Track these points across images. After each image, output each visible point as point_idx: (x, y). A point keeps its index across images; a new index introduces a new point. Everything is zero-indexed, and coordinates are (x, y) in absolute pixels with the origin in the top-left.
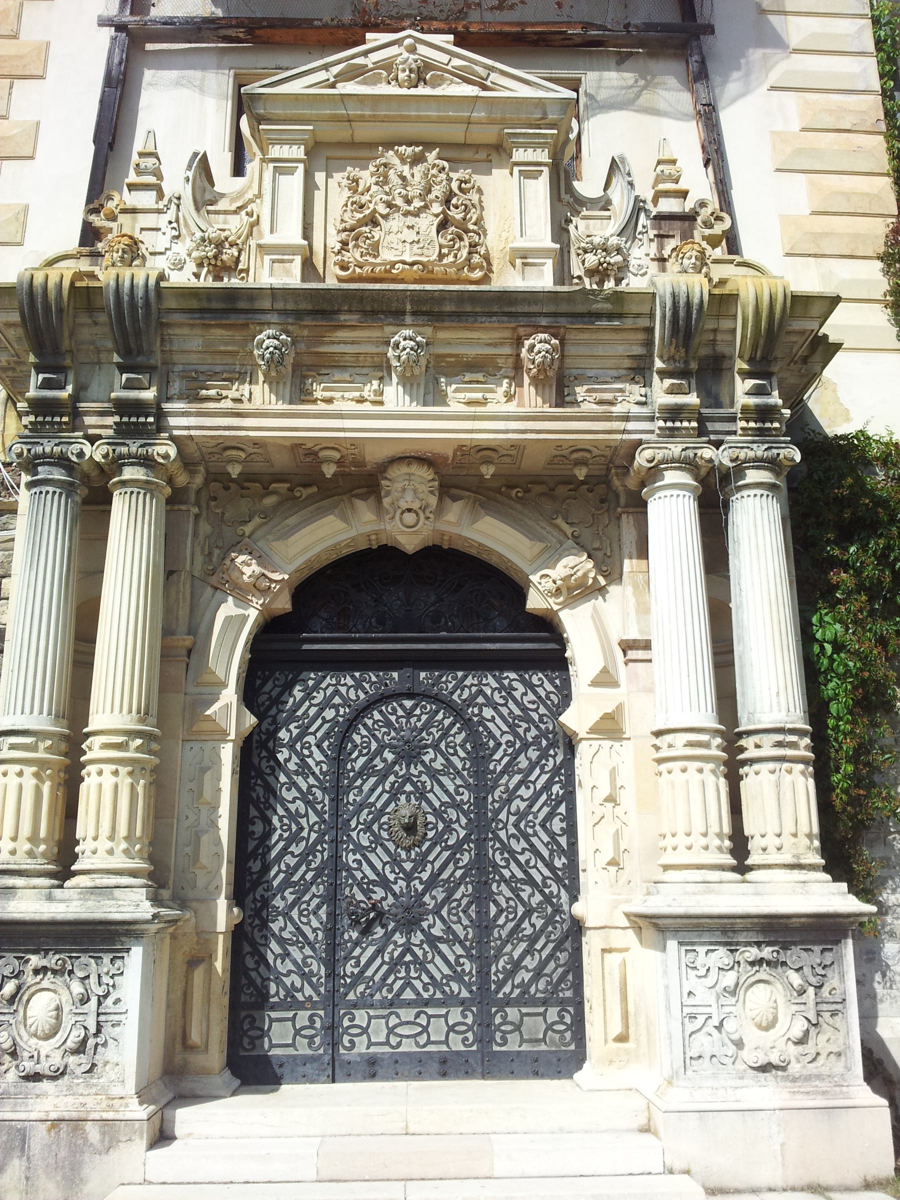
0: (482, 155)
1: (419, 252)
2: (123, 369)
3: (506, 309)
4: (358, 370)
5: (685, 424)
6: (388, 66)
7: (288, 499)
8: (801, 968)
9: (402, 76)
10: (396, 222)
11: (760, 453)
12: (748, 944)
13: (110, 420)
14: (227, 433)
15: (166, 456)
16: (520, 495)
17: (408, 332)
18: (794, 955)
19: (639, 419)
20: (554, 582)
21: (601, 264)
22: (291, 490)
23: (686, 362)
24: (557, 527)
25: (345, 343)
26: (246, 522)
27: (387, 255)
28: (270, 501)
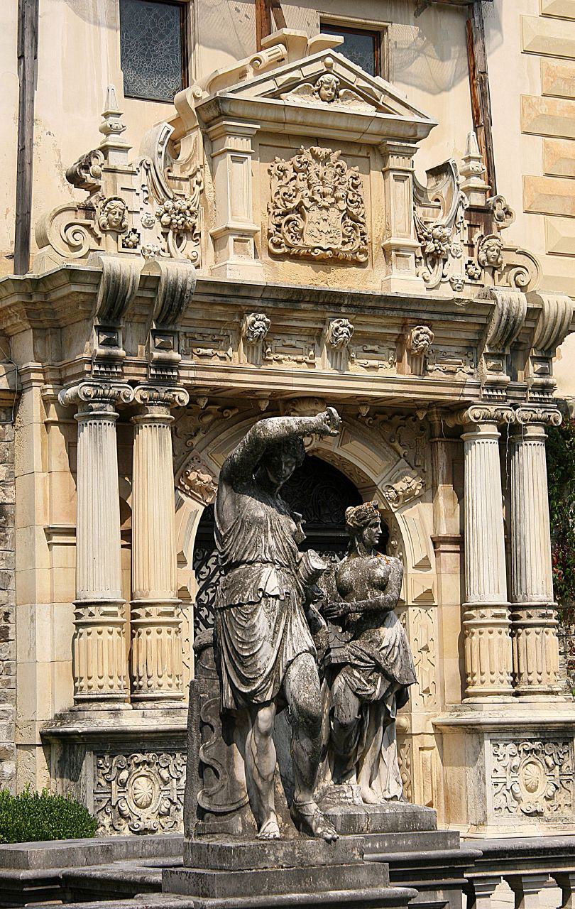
0: (363, 153)
1: (331, 240)
2: (156, 333)
3: (404, 307)
4: (298, 338)
5: (499, 393)
6: (314, 79)
7: (218, 418)
8: (552, 754)
9: (324, 92)
10: (314, 214)
11: (540, 416)
12: (526, 740)
13: (144, 371)
14: (219, 384)
15: (181, 401)
16: (371, 422)
17: (345, 321)
18: (550, 748)
19: (470, 386)
20: (396, 492)
21: (436, 250)
22: (221, 410)
23: (504, 349)
24: (396, 451)
25: (296, 320)
26: (192, 437)
27: (309, 241)
28: (207, 419)
